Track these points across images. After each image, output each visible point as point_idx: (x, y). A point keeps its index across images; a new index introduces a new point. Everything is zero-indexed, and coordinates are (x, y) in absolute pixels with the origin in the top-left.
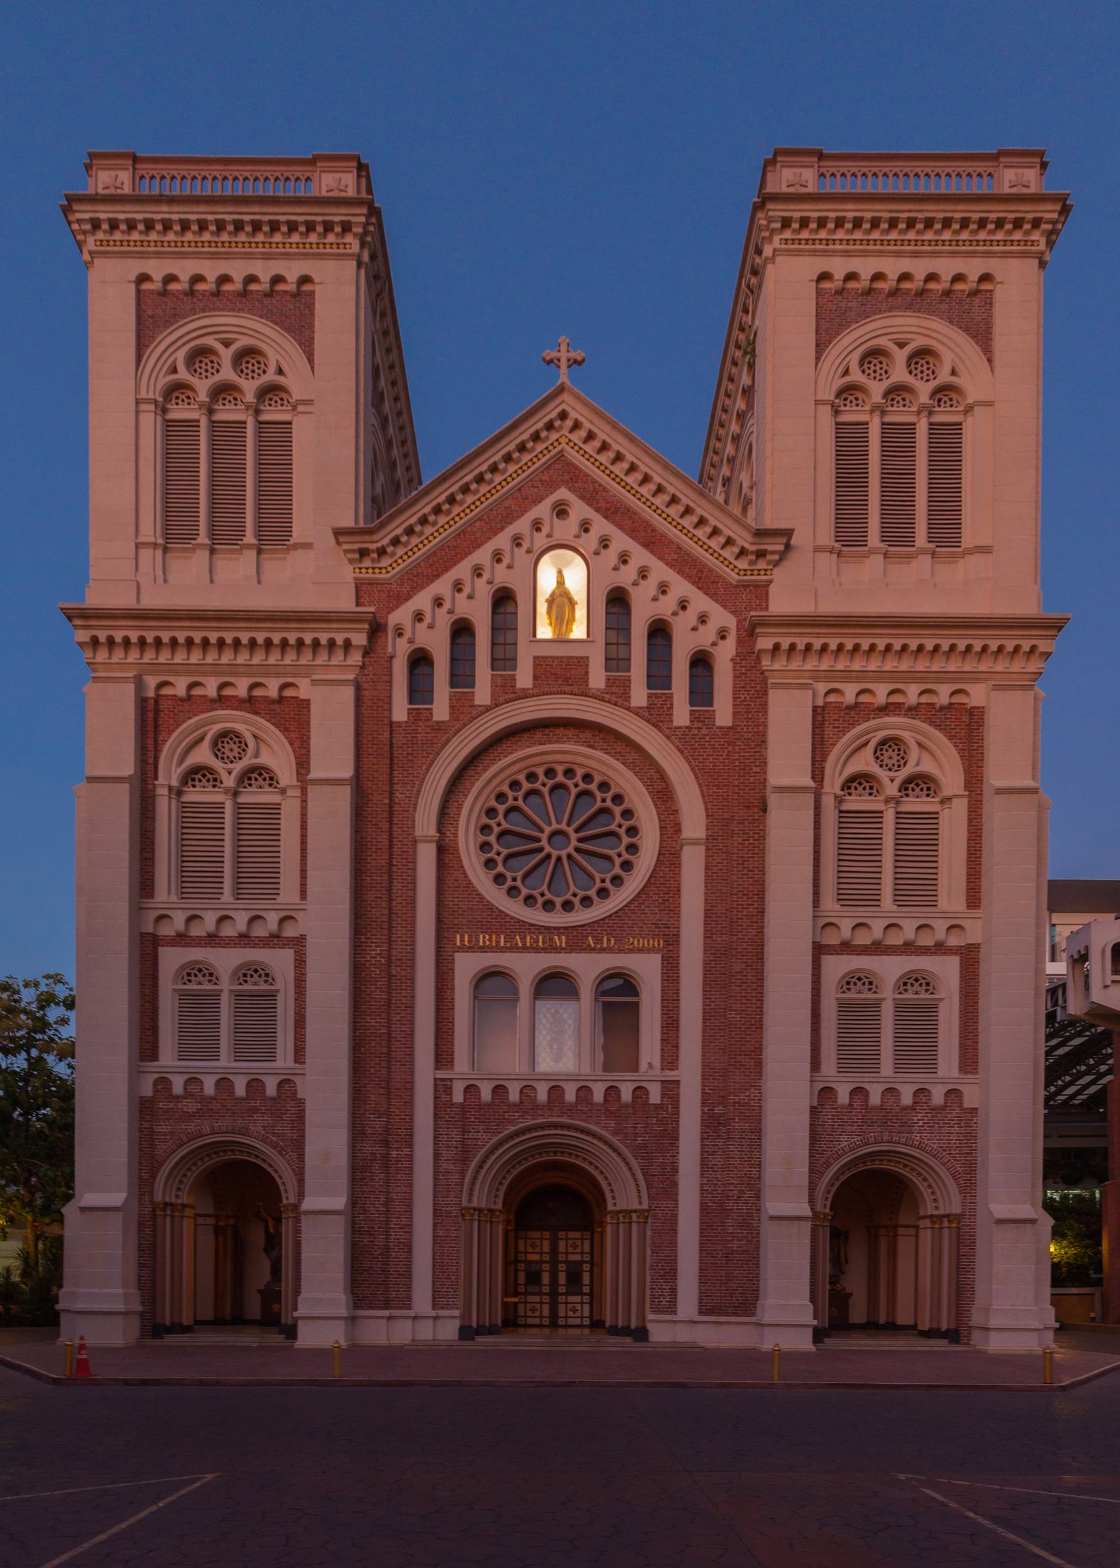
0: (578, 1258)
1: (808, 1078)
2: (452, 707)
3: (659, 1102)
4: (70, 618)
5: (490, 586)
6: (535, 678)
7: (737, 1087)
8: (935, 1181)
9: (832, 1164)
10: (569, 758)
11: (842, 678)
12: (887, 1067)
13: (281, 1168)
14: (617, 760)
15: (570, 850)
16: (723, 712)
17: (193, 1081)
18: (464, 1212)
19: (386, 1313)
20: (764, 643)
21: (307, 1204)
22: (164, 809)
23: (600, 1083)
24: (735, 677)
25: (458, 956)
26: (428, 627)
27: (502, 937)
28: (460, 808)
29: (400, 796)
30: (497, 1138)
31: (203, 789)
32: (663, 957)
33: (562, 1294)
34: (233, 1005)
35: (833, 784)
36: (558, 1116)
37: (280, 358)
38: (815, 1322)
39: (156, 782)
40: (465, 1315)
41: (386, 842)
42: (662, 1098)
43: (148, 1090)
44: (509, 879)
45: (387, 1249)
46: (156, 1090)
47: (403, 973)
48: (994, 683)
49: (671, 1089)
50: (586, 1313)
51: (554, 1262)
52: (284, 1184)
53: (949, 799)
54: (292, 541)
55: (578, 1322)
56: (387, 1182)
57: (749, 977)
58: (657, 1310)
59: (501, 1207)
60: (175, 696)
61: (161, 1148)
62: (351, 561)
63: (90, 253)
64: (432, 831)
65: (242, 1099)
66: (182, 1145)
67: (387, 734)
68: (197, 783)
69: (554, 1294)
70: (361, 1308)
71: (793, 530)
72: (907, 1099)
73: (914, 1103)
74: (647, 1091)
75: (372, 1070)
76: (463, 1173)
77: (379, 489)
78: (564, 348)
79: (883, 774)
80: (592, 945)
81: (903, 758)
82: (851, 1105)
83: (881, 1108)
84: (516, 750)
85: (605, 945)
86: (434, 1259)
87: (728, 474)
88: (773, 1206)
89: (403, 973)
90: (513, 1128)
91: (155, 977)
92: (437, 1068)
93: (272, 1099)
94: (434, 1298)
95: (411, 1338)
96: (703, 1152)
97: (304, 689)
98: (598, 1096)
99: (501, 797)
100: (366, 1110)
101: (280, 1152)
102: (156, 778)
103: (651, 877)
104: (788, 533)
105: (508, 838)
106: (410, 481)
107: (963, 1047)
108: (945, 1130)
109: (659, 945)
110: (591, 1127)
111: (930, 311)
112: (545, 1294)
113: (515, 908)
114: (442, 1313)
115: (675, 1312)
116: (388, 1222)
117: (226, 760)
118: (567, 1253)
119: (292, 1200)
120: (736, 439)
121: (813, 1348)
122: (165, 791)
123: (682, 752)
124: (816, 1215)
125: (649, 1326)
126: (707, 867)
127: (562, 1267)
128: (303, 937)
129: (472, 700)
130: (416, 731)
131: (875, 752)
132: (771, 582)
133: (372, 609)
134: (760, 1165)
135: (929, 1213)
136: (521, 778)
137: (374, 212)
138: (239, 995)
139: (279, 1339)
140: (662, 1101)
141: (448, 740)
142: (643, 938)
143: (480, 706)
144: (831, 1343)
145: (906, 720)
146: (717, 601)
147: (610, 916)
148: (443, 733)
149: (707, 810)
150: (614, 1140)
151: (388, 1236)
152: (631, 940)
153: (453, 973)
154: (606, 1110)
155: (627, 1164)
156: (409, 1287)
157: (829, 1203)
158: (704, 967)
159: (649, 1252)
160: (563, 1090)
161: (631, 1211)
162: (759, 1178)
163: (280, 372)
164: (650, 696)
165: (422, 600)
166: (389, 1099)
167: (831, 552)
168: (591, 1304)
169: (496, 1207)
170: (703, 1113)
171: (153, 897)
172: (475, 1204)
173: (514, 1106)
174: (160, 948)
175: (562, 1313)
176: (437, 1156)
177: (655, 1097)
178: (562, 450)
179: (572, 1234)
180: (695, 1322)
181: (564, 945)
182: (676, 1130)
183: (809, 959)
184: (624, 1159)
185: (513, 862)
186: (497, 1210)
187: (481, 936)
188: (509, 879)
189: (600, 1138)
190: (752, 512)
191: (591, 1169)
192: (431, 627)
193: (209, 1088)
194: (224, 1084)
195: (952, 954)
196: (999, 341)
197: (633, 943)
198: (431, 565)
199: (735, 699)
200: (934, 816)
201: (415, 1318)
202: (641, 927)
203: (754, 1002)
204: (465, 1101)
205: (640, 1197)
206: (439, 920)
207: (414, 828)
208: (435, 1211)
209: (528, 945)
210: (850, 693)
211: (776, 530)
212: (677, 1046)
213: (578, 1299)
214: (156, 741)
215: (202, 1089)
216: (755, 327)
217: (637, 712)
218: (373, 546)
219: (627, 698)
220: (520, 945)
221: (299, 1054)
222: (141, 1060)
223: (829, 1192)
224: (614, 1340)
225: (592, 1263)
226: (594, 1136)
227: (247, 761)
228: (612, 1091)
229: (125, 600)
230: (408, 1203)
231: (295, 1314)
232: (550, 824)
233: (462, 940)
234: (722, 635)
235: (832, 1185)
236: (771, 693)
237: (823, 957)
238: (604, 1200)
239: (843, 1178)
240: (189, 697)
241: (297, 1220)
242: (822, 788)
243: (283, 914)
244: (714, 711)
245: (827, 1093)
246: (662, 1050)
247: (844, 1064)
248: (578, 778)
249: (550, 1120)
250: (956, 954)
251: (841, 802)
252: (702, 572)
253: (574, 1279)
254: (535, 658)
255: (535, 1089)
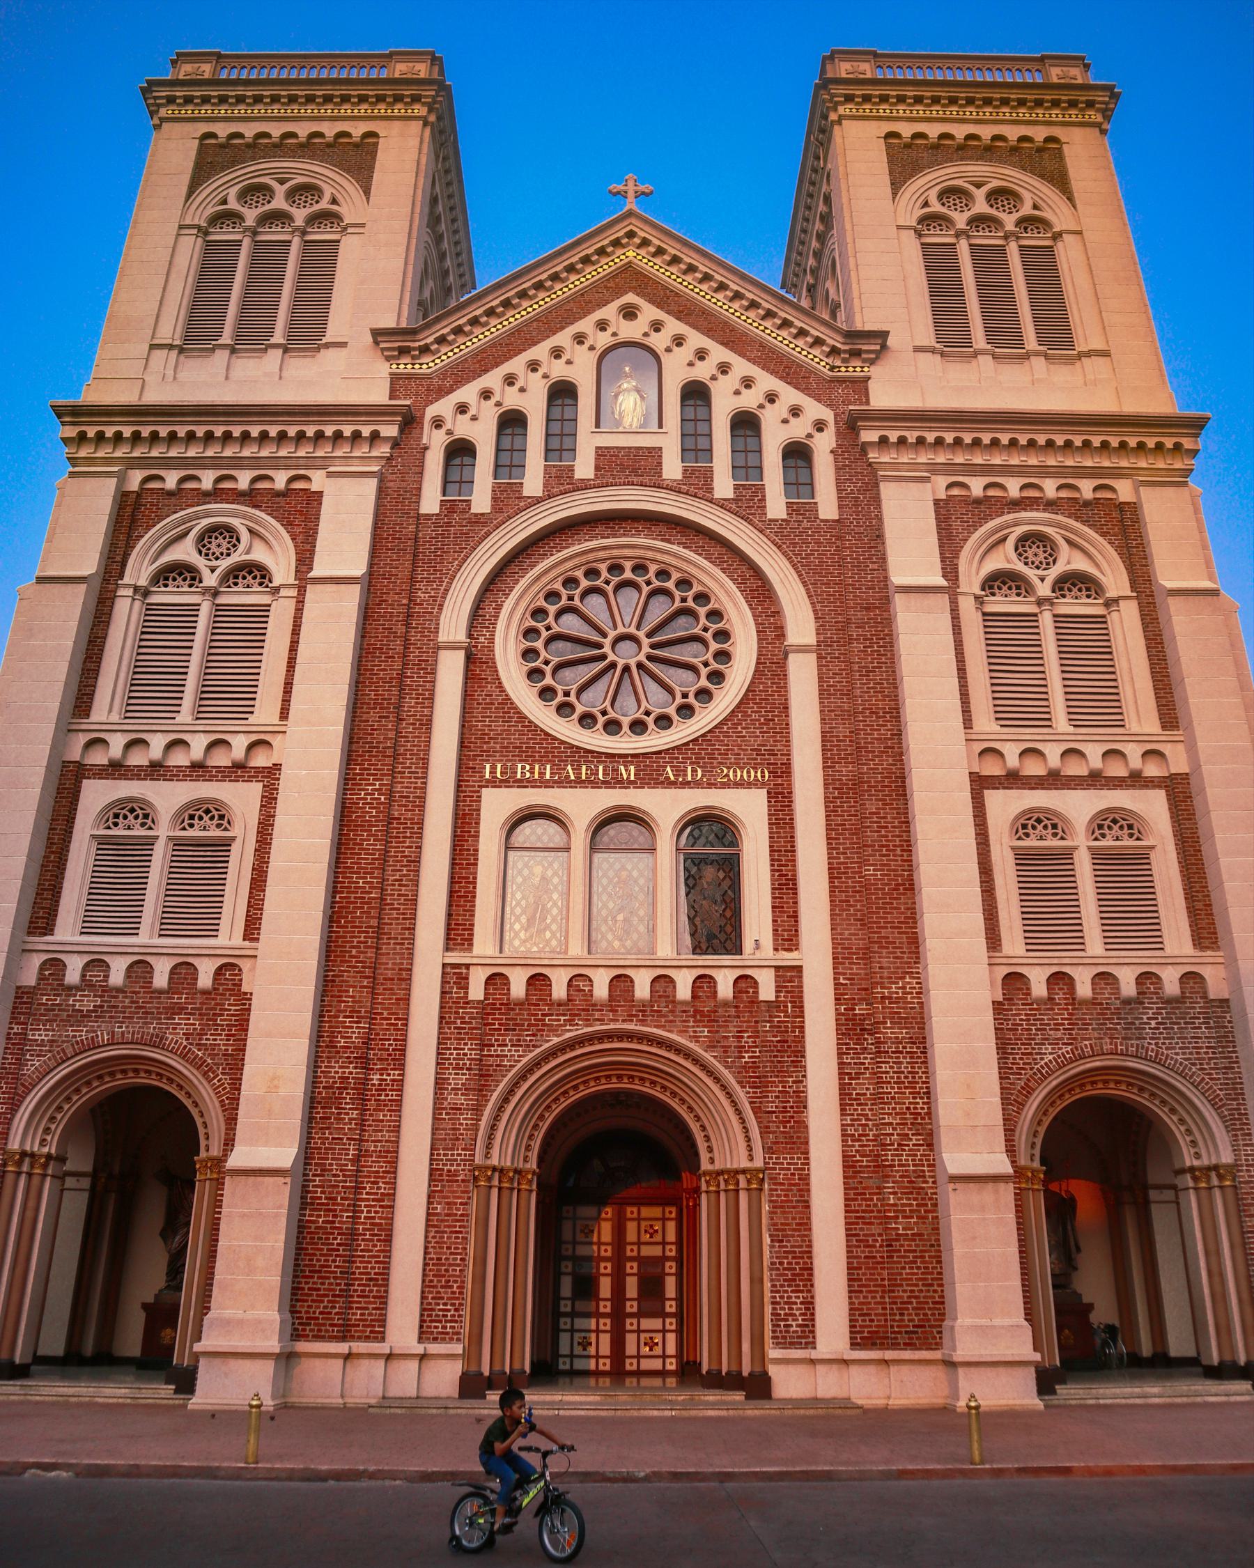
0: (656, 1251)
1: (986, 961)
2: (495, 499)
3: (774, 999)
4: (59, 416)
5: (545, 381)
6: (597, 468)
7: (886, 975)
8: (1188, 1113)
9: (1034, 1090)
10: (641, 553)
11: (963, 471)
12: (1095, 944)
13: (207, 1097)
14: (700, 555)
15: (642, 657)
16: (828, 506)
17: (97, 964)
18: (478, 1174)
19: (343, 1348)
20: (869, 436)
21: (236, 1160)
22: (126, 612)
23: (685, 970)
24: (838, 469)
25: (485, 792)
26: (472, 419)
27: (548, 767)
28: (498, 608)
29: (422, 595)
30: (531, 1055)
31: (176, 589)
32: (768, 793)
33: (632, 1315)
34: (169, 857)
35: (971, 581)
36: (623, 1021)
37: (334, 192)
38: (1037, 1357)
39: (120, 582)
40: (472, 1354)
41: (400, 649)
42: (776, 991)
43: (29, 978)
44: (560, 693)
45: (353, 1235)
46: (41, 978)
47: (409, 815)
48: (1141, 479)
49: (790, 978)
50: (671, 1349)
51: (619, 1260)
52: (205, 1125)
53: (1116, 601)
54: (324, 340)
55: (656, 1364)
56: (362, 1123)
57: (889, 820)
58: (784, 1341)
59: (534, 1166)
60: (163, 489)
61: (33, 1064)
62: (388, 359)
63: (160, 119)
64: (461, 636)
65: (161, 992)
66: (64, 1062)
67: (412, 528)
68: (170, 582)
69: (618, 1316)
70: (305, 1337)
71: (888, 332)
72: (1128, 988)
73: (1138, 993)
74: (756, 982)
75: (354, 952)
76: (478, 1110)
77: (427, 294)
78: (631, 184)
79: (1031, 573)
80: (672, 778)
81: (1051, 555)
82: (1050, 999)
83: (1093, 1002)
84: (574, 544)
85: (689, 778)
86: (426, 1253)
87: (812, 281)
88: (955, 1160)
89: (409, 815)
90: (556, 1040)
91: (70, 820)
92: (447, 949)
93: (205, 992)
94: (422, 1321)
95: (381, 1394)
96: (841, 1075)
97: (318, 481)
98: (684, 991)
99: (552, 596)
100: (339, 1011)
101: (205, 1074)
102: (121, 576)
103: (748, 690)
104: (883, 335)
105: (560, 645)
106: (463, 286)
107: (1193, 912)
108: (1190, 1033)
109: (763, 777)
110: (674, 1037)
111: (1001, 161)
112: (605, 1315)
113: (567, 730)
114: (434, 1348)
115: (812, 1345)
116: (358, 1188)
117: (210, 557)
118: (639, 1243)
119: (215, 1151)
120: (818, 255)
121: (1036, 1403)
122: (130, 592)
123: (779, 547)
124: (1019, 1173)
125: (773, 1370)
126: (821, 679)
127: (632, 1267)
128: (277, 767)
129: (520, 491)
130: (449, 525)
131: (1016, 549)
132: (869, 378)
133: (408, 402)
134: (928, 1093)
135: (1188, 1164)
136: (579, 574)
137: (443, 88)
138: (177, 843)
139: (164, 1392)
140: (777, 997)
141: (488, 534)
142: (742, 768)
143: (529, 497)
144: (1069, 1392)
145: (1047, 515)
146: (809, 395)
147: (696, 740)
148: (481, 526)
149: (815, 611)
150: (708, 1057)
151: (355, 1218)
152: (725, 771)
153: (479, 815)
154: (695, 1011)
155: (729, 1095)
156: (383, 1301)
157: (1037, 1151)
158: (826, 807)
159: (767, 1240)
160: (632, 981)
161: (737, 1172)
162: (929, 1114)
163: (334, 201)
164: (736, 487)
165: (468, 393)
166: (374, 994)
167: (933, 352)
168: (679, 1332)
169: (528, 1166)
170: (838, 1014)
171: (88, 716)
172: (495, 1161)
173: (559, 1005)
174: (85, 781)
175: (631, 1349)
176: (440, 1084)
177: (767, 991)
178: (630, 262)
179: (646, 1212)
180: (846, 1362)
181: (632, 778)
182: (801, 1040)
183: (967, 795)
184: (724, 1087)
185: (567, 673)
186: (528, 1172)
187: (520, 766)
188: (560, 693)
189: (688, 1054)
190: (841, 316)
191: (674, 1104)
192: (474, 418)
193: (117, 977)
194: (140, 969)
195: (1154, 787)
196: (1076, 186)
197: (727, 775)
198: (479, 361)
199: (839, 491)
200: (1101, 620)
201: (389, 1357)
202: (739, 754)
203: (899, 852)
204: (485, 999)
205: (750, 1148)
206: (463, 745)
207: (438, 632)
208: (432, 1172)
209: (584, 777)
210: (977, 486)
211: (869, 331)
212: (795, 916)
213: (656, 1323)
214: (129, 536)
215: (107, 976)
216: (827, 169)
217: (722, 504)
218: (417, 344)
219: (709, 488)
220: (573, 778)
221: (252, 929)
222: (30, 933)
223: (1035, 1134)
224: (712, 1396)
225: (679, 1260)
226: (678, 1049)
227: (236, 558)
228: (704, 983)
229: (125, 396)
230: (391, 1157)
231: (197, 1347)
232: (615, 627)
233: (493, 772)
234: (820, 426)
235: (1039, 1123)
236: (882, 485)
237: (986, 792)
238: (697, 1154)
239: (1053, 1112)
240: (180, 490)
241: (220, 1184)
242: (958, 587)
243: (254, 737)
244: (816, 503)
245: (1014, 982)
246: (774, 921)
247: (1035, 937)
248: (651, 574)
249: (612, 1026)
250: (1160, 787)
251: (982, 603)
252: (790, 368)
253: (651, 1288)
254: (597, 448)
255: (590, 980)
